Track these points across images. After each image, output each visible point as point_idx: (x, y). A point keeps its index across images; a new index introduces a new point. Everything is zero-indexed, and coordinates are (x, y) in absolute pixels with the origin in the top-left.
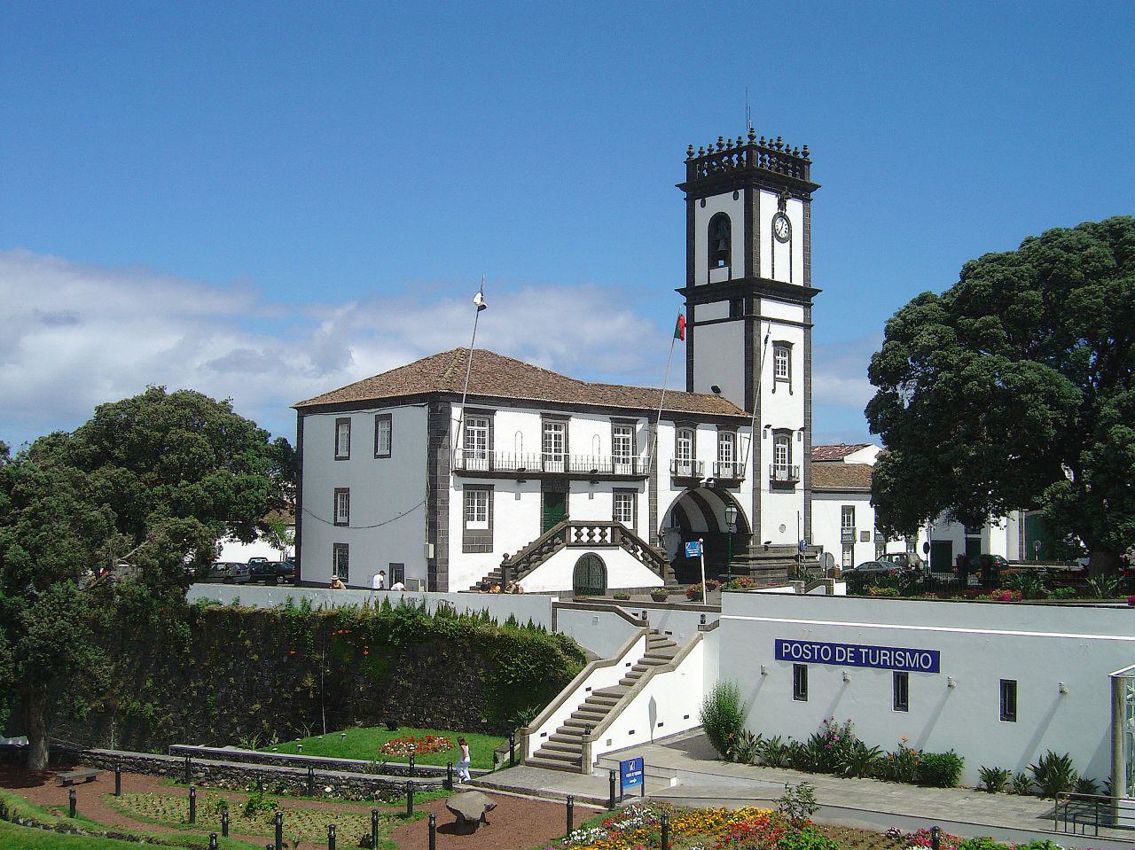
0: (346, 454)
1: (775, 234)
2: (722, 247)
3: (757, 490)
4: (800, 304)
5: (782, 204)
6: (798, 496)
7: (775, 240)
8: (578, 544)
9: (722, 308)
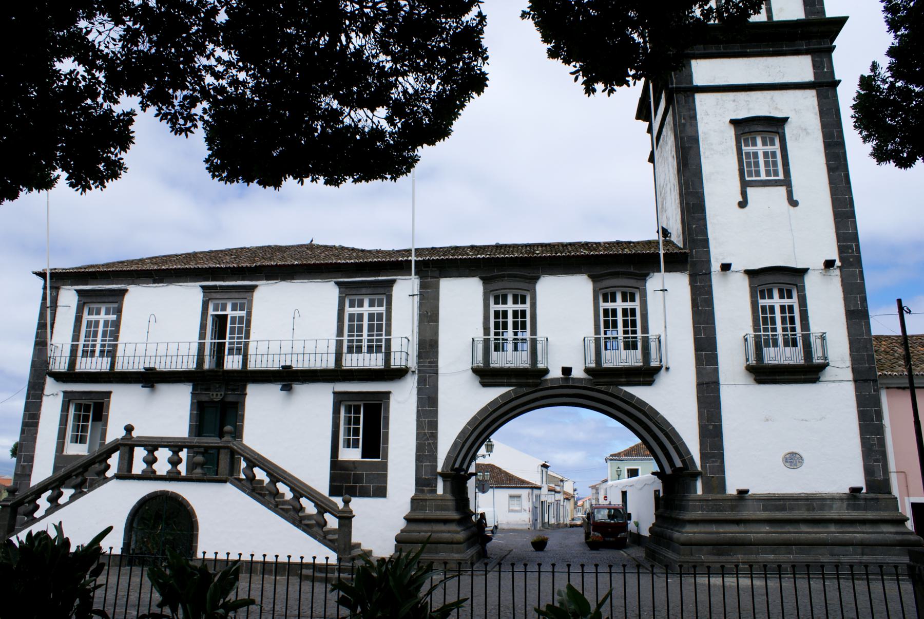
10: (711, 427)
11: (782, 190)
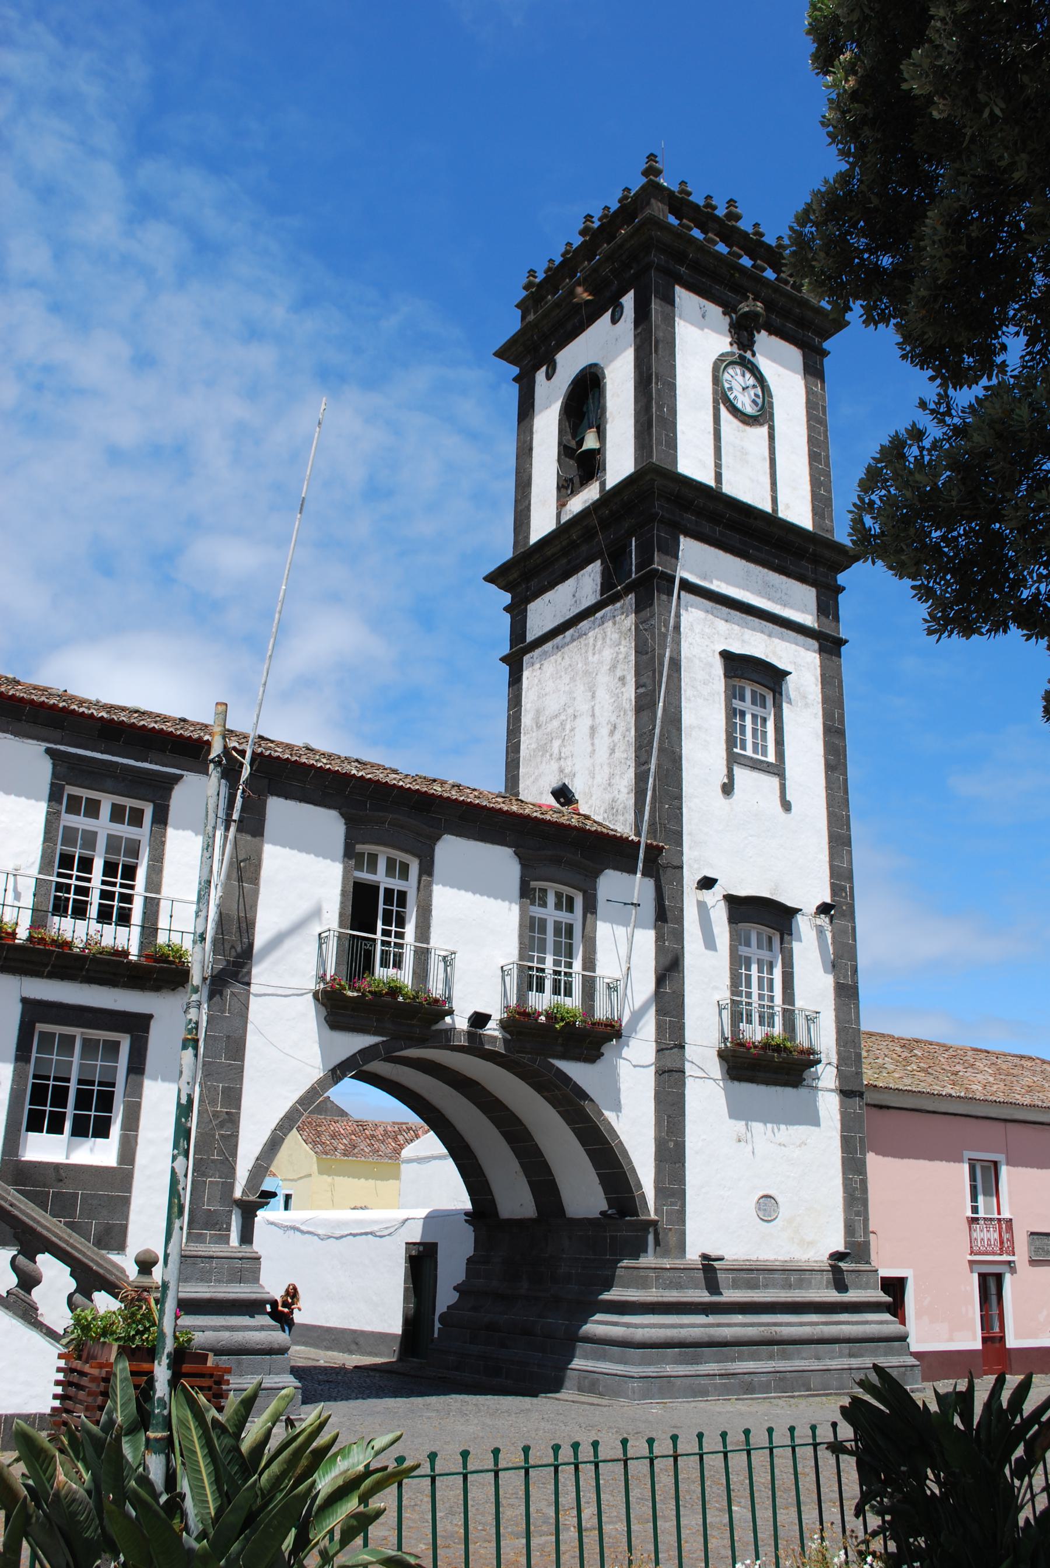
1: (722, 398)
3: (670, 1080)
7: (724, 412)
9: (587, 583)
10: (671, 1145)
11: (775, 781)
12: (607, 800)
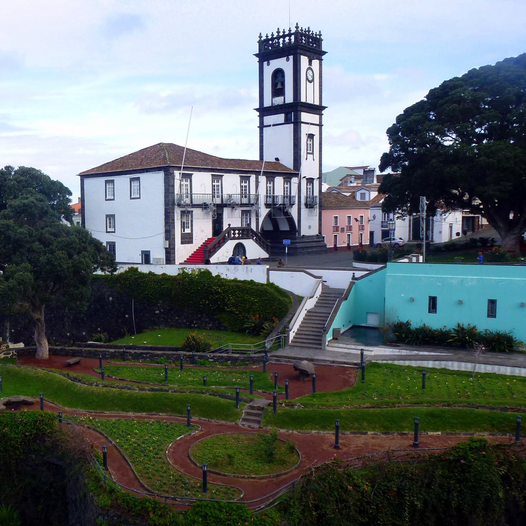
0: (112, 198)
1: (307, 79)
2: (279, 86)
4: (317, 114)
5: (310, 63)
6: (317, 211)
7: (308, 82)
8: (234, 238)
9: (280, 118)
12: (288, 162)
